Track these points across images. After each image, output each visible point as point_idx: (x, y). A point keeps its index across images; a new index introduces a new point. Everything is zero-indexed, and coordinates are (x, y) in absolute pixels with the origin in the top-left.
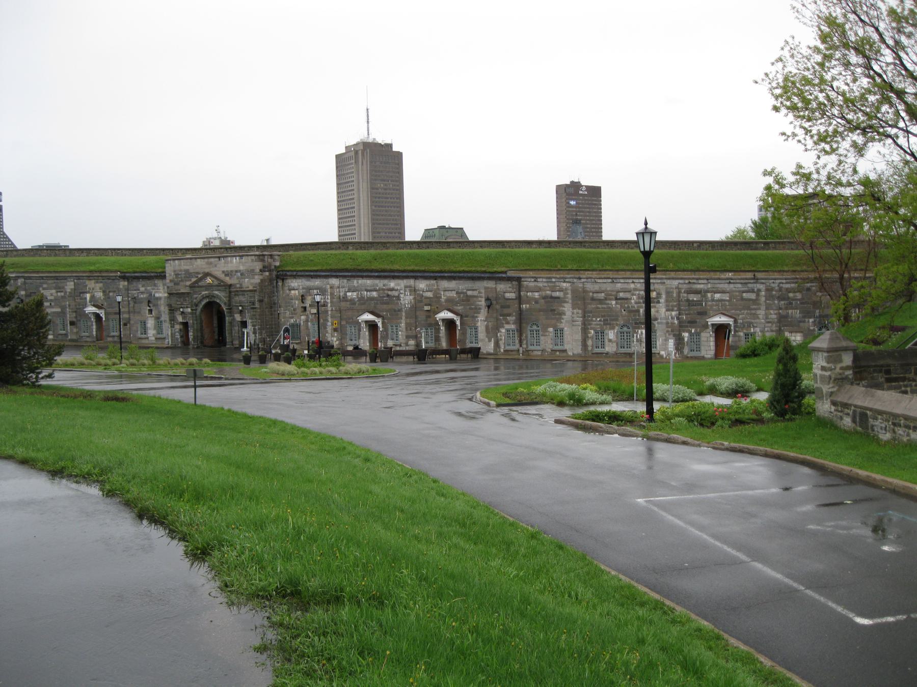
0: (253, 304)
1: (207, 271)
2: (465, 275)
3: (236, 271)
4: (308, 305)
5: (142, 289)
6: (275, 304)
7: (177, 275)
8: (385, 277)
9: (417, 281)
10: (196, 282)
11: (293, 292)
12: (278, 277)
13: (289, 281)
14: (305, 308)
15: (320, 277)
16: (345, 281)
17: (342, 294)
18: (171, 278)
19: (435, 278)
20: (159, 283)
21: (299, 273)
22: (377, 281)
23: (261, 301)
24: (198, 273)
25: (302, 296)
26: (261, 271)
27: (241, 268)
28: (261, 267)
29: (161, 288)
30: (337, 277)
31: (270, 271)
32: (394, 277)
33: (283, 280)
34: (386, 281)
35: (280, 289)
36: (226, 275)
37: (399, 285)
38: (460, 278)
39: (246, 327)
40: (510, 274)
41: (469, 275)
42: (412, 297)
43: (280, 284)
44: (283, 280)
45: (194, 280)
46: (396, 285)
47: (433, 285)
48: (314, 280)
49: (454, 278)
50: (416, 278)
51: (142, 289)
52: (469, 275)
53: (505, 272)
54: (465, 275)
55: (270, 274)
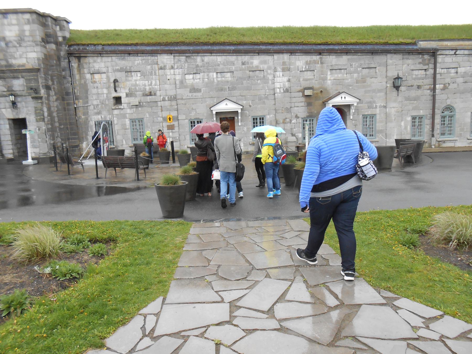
0: (36, 91)
2: (363, 47)
4: (123, 95)
6: (68, 94)
8: (246, 52)
9: (293, 57)
11: (97, 76)
12: (70, 54)
13: (91, 60)
14: (118, 100)
15: (143, 53)
16: (183, 58)
17: (178, 77)
19: (320, 53)
21: (107, 48)
22: (232, 58)
23: (48, 88)
25: (115, 81)
26: (43, 40)
28: (43, 35)
30: (170, 52)
31: (57, 43)
32: (260, 52)
33: (79, 58)
34: (246, 58)
35: (75, 71)
37: (265, 62)
38: (356, 52)
39: (25, 127)
40: (423, 44)
41: (369, 47)
42: (285, 79)
43: (74, 64)
44: (79, 58)
46: (262, 62)
47: (315, 62)
48: (132, 58)
49: (347, 52)
50: (292, 52)
52: (369, 47)
53: (415, 44)
54: (363, 47)
55: (58, 50)
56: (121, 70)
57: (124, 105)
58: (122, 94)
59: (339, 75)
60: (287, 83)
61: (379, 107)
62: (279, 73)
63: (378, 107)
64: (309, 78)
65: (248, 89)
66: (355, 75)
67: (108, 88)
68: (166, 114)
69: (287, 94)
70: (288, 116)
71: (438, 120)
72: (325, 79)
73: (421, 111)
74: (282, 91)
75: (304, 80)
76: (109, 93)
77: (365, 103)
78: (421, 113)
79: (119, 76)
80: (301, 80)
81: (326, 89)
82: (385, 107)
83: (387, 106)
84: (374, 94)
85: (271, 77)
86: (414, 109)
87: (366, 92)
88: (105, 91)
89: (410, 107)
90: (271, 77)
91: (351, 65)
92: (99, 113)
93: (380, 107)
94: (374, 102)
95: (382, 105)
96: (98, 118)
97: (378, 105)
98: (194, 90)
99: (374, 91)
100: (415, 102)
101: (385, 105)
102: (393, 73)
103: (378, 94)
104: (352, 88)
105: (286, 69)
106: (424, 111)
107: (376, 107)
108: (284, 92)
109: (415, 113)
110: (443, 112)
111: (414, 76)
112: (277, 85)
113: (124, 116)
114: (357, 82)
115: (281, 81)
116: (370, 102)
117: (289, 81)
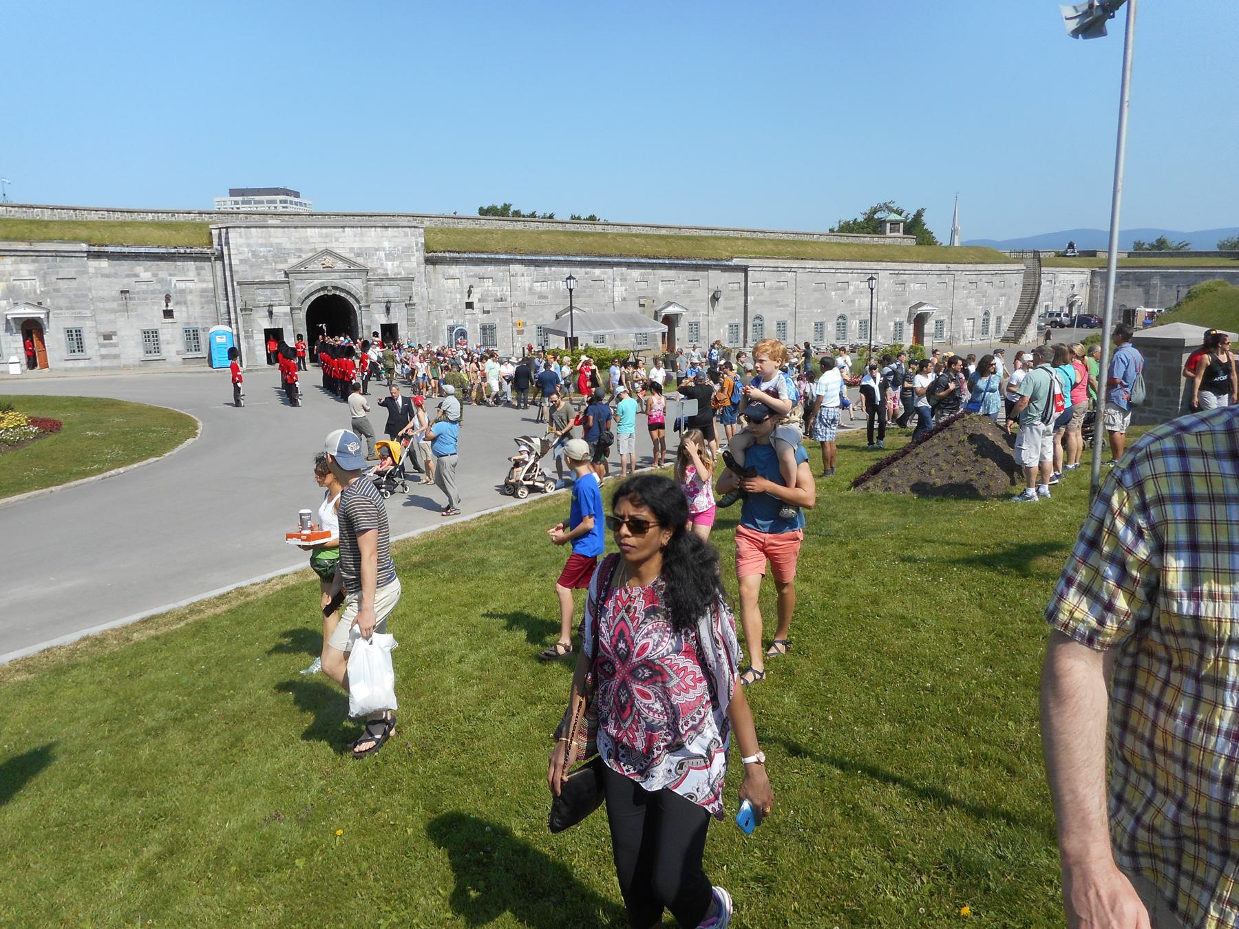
1: (321, 247)
3: (377, 250)
5: (145, 275)
7: (254, 254)
10: (302, 264)
14: (470, 305)
17: (527, 285)
18: (241, 257)
20: (191, 265)
24: (300, 250)
25: (471, 287)
27: (386, 245)
29: (192, 274)
36: (358, 255)
45: (293, 261)
51: (145, 275)
56: (475, 276)
57: (476, 311)
58: (474, 299)
59: (669, 285)
62: (618, 283)
65: (590, 296)
67: (462, 293)
68: (516, 320)
71: (750, 327)
76: (462, 298)
78: (737, 321)
79: (472, 281)
85: (610, 286)
88: (458, 296)
90: (610, 286)
92: (451, 317)
96: (451, 322)
98: (542, 296)
102: (713, 286)
105: (623, 280)
106: (739, 320)
109: (732, 322)
112: (616, 294)
113: (475, 321)
115: (619, 291)
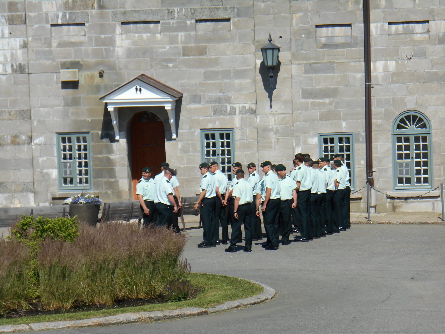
59: (142, 35)
60: (19, 53)
61: (240, 112)
63: (237, 112)
64: (73, 40)
66: (181, 35)
69: (21, 77)
70: (25, 127)
72: (111, 42)
73: (344, 124)
74: (9, 70)
75: (60, 45)
77: (207, 102)
78: (344, 127)
80: (55, 44)
81: (112, 67)
82: (253, 112)
83: (258, 112)
84: (226, 81)
86: (325, 117)
87: (207, 76)
89: (316, 113)
91: (170, 13)
93: (243, 111)
94: (228, 100)
95: (247, 106)
97: (237, 106)
99: (226, 74)
100: (327, 101)
101: (254, 107)
103: (237, 82)
104: (174, 67)
107: (233, 112)
108: (15, 71)
109: (329, 129)
110: (399, 127)
111: (323, 40)
114: (186, 52)
116: (219, 100)
117: (25, 46)
